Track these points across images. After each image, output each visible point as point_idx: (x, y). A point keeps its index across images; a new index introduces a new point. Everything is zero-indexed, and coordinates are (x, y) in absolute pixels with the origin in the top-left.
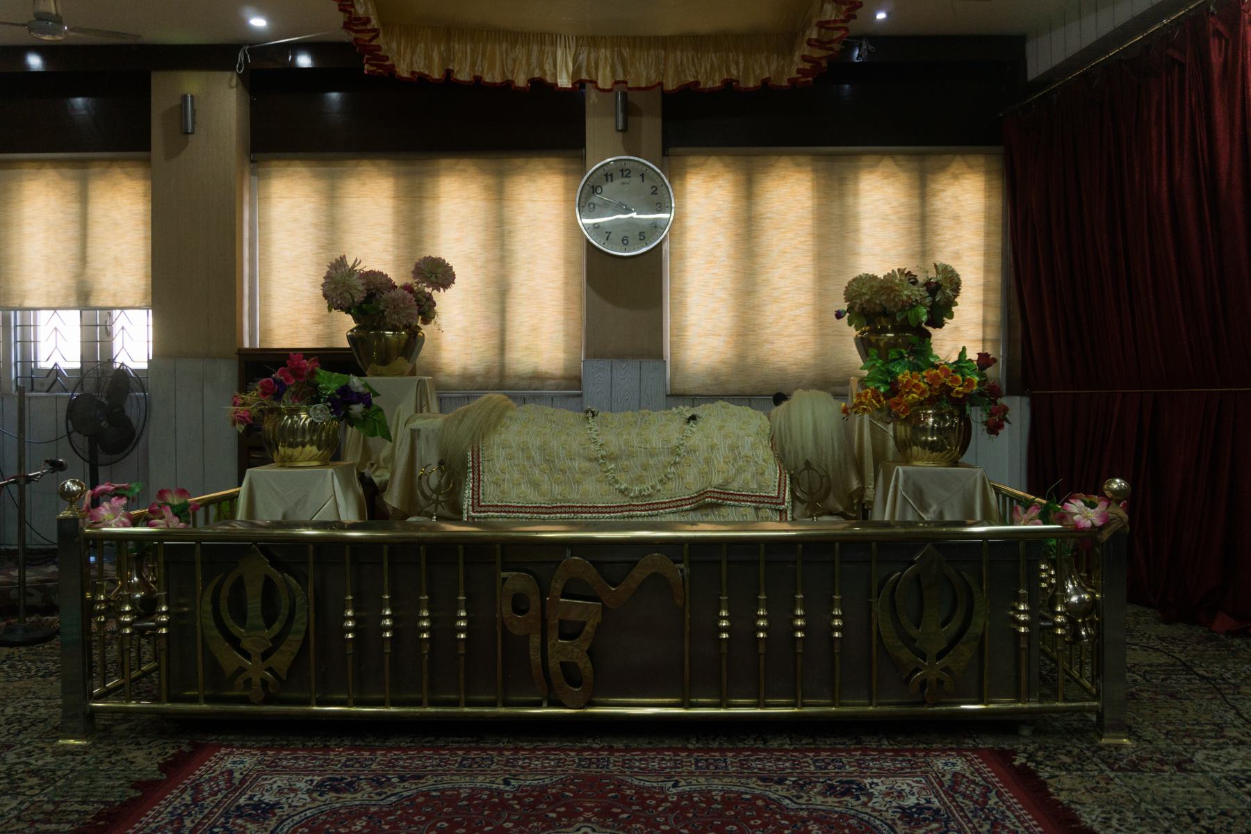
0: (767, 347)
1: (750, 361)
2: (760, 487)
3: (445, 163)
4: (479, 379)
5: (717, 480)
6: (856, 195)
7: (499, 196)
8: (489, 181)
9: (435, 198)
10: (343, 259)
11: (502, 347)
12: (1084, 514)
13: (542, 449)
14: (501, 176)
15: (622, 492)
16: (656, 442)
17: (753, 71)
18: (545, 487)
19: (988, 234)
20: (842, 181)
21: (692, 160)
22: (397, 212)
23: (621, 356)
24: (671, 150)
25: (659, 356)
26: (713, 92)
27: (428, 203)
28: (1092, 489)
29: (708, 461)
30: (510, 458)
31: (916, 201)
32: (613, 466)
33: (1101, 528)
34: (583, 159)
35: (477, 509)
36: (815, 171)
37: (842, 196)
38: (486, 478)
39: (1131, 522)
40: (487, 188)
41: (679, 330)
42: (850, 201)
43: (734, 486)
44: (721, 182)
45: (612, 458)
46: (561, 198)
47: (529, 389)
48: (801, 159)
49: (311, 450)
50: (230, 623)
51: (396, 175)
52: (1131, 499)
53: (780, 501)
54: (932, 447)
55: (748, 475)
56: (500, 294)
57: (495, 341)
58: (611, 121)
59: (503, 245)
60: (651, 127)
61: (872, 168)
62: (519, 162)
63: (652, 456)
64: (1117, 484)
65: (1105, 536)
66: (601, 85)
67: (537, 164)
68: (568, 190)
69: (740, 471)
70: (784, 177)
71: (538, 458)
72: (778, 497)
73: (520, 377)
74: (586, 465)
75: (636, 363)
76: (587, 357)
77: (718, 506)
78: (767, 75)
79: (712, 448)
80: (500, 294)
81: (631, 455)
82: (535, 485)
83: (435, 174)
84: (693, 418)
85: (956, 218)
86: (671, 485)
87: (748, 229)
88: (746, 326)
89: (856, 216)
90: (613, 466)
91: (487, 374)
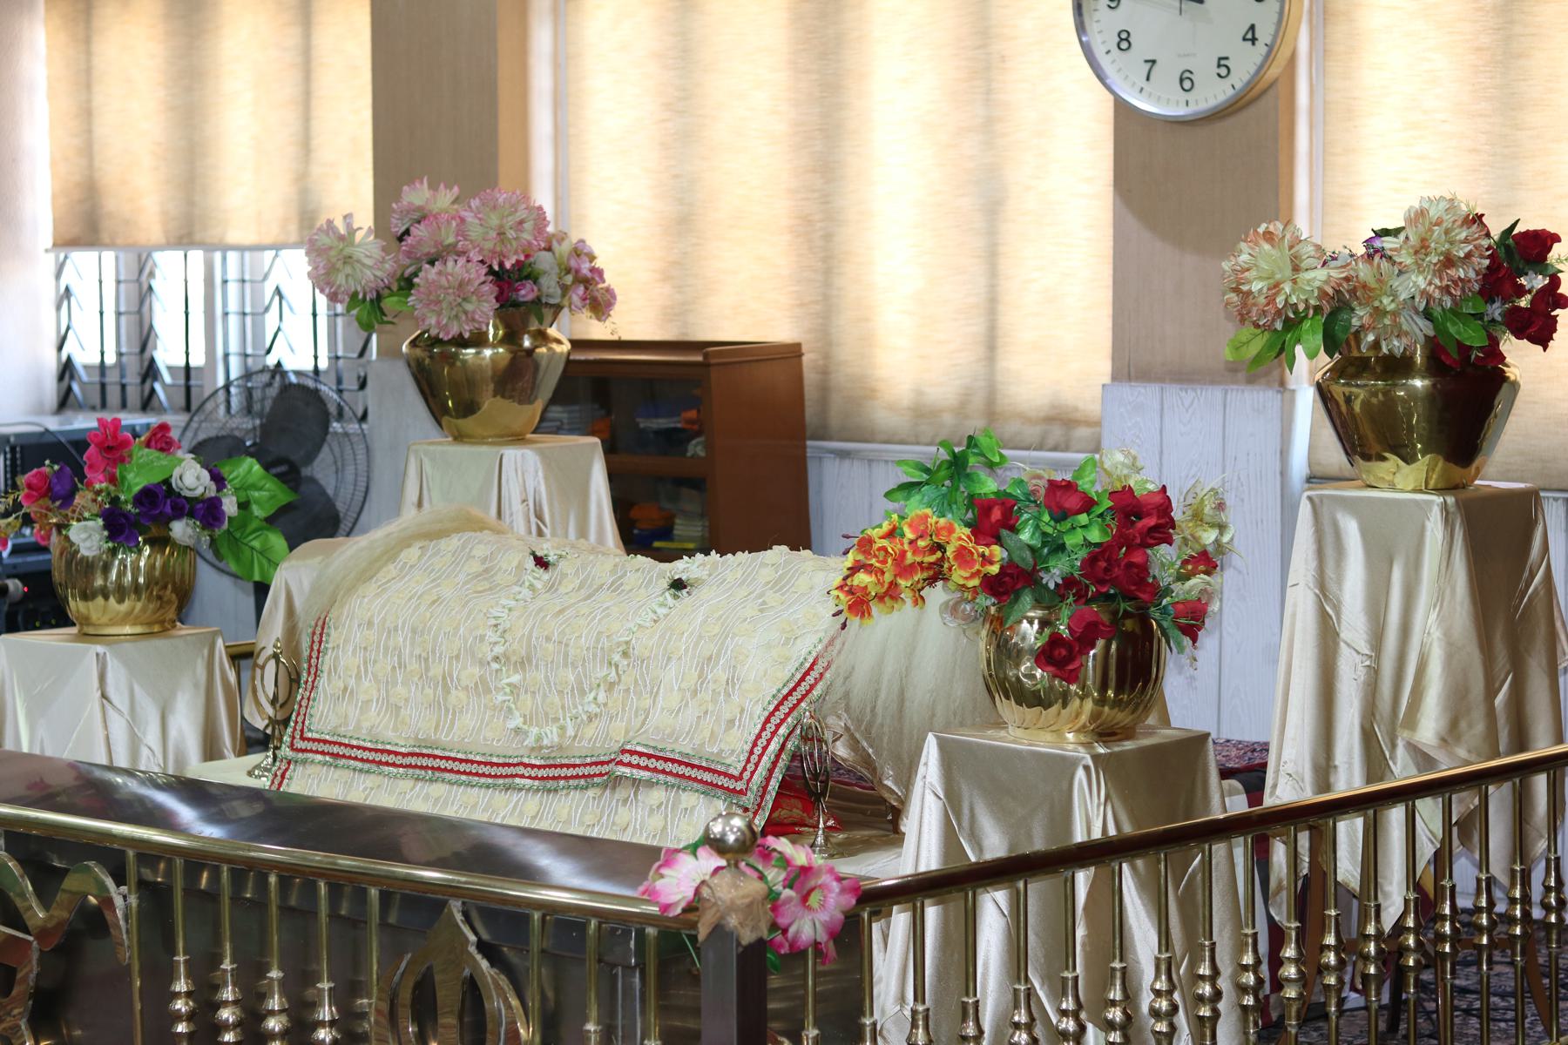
4: (948, 419)
11: (991, 344)
32: (516, 678)
35: (300, 744)
47: (1040, 448)
53: (740, 786)
56: (987, 210)
57: (978, 327)
59: (989, 92)
72: (740, 778)
73: (1026, 419)
75: (1214, 394)
76: (1116, 377)
77: (650, 784)
80: (987, 210)
84: (678, 585)
90: (516, 678)
91: (961, 409)
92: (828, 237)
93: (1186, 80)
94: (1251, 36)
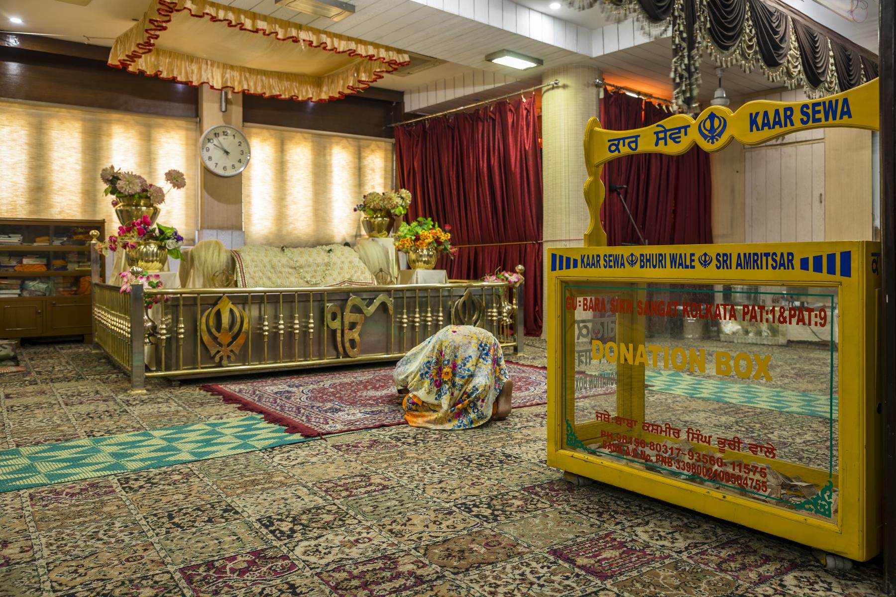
0: (291, 226)
1: (284, 232)
2: (365, 279)
3: (115, 116)
5: (347, 277)
6: (331, 155)
7: (147, 139)
8: (143, 129)
9: (110, 135)
10: (112, 167)
12: (513, 278)
13: (270, 261)
14: (149, 126)
15: (307, 282)
16: (319, 260)
17: (307, 93)
18: (274, 280)
19: (385, 178)
20: (325, 148)
21: (254, 130)
22: (84, 141)
23: (221, 228)
24: (246, 124)
25: (241, 229)
26: (285, 100)
27: (104, 138)
28: (513, 271)
29: (341, 268)
30: (256, 266)
31: (357, 161)
33: (516, 283)
34: (199, 124)
36: (312, 142)
37: (325, 155)
38: (247, 276)
39: (525, 280)
40: (141, 133)
41: (249, 216)
42: (328, 158)
43: (354, 279)
44: (268, 142)
45: (301, 267)
46: (184, 142)
48: (306, 135)
49: (157, 265)
50: (213, 330)
51: (84, 120)
52: (524, 274)
54: (425, 262)
55: (359, 274)
58: (217, 106)
60: (237, 111)
61: (338, 143)
62: (160, 121)
63: (318, 266)
64: (520, 267)
65: (518, 285)
66: (215, 87)
67: (170, 122)
68: (187, 138)
69: (356, 272)
70: (298, 144)
71: (269, 266)
74: (291, 270)
75: (230, 232)
78: (310, 96)
79: (343, 263)
81: (309, 266)
82: (269, 279)
83: (109, 122)
84: (330, 251)
85: (373, 170)
86: (328, 279)
87: (281, 167)
88: (281, 216)
89: (331, 165)
92: (95, 196)
93: (225, 168)
94: (240, 161)
